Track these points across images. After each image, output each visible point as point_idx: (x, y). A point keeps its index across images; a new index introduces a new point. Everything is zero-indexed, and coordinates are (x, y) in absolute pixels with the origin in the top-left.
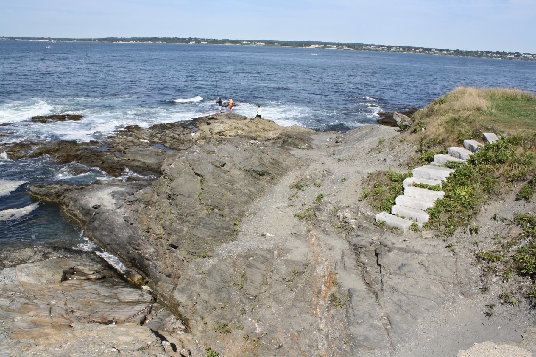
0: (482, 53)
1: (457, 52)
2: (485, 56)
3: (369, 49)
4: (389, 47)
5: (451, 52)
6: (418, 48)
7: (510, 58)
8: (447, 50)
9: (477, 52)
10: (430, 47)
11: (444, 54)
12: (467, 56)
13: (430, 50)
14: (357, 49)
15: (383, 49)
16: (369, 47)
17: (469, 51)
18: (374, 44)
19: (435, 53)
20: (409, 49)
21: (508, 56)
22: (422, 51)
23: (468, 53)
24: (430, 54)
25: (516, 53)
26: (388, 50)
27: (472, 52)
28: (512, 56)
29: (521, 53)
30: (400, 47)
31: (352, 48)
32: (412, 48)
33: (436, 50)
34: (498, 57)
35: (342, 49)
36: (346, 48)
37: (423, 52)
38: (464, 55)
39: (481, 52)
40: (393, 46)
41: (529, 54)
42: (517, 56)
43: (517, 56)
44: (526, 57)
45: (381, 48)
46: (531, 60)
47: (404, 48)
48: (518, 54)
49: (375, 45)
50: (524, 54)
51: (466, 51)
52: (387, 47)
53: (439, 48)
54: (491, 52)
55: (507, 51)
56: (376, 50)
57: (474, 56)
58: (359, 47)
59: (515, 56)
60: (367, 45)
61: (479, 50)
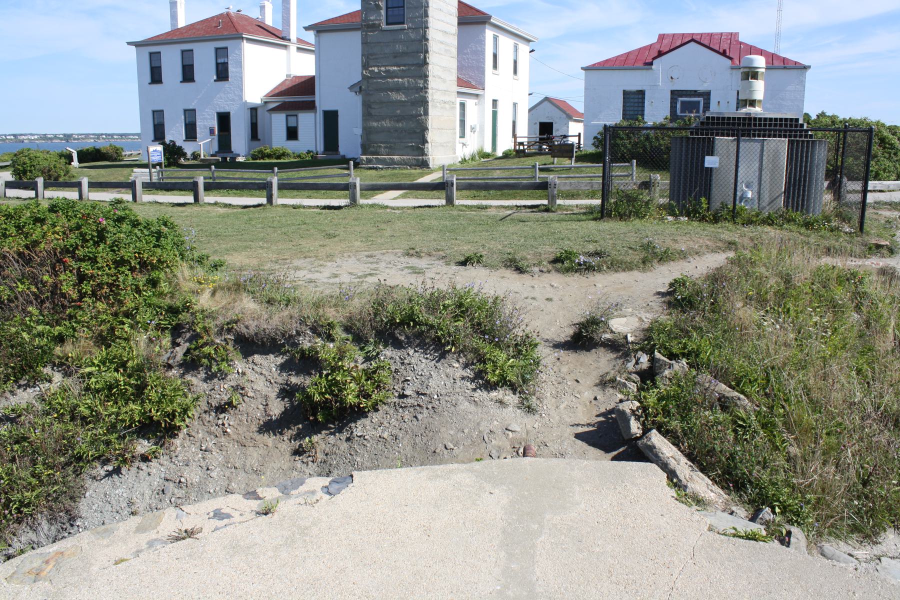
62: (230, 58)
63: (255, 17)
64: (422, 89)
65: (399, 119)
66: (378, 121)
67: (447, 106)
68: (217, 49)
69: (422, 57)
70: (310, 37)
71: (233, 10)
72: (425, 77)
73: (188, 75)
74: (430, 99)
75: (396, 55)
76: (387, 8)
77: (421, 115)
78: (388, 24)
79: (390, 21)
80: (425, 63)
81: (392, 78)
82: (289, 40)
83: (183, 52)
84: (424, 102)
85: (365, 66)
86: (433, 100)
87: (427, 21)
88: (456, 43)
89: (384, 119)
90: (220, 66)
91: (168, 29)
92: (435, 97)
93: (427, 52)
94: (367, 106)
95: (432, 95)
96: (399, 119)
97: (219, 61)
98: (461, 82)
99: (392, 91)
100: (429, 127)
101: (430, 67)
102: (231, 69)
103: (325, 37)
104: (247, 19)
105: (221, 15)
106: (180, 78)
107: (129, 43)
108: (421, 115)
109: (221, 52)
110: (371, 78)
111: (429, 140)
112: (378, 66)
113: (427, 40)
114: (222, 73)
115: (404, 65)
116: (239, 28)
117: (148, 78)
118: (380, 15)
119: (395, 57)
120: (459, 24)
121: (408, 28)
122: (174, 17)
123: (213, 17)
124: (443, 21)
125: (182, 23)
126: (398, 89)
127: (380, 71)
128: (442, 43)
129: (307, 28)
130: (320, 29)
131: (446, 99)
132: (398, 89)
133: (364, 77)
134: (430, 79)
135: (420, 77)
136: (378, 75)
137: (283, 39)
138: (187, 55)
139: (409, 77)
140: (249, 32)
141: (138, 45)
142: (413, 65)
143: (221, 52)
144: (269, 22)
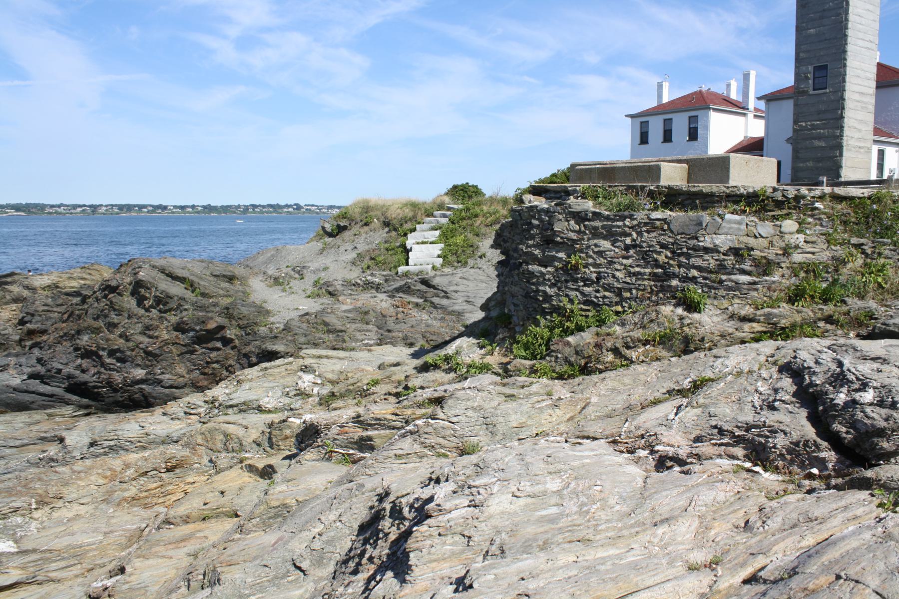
0: (246, 208)
1: (208, 209)
2: (251, 213)
3: (57, 213)
4: (94, 208)
5: (200, 208)
6: (145, 206)
7: (288, 212)
8: (193, 207)
9: (239, 206)
10: (164, 204)
11: (188, 212)
12: (224, 213)
13: (164, 208)
14: (35, 213)
15: (83, 210)
16: (57, 209)
17: (227, 206)
18: (65, 203)
19: (173, 213)
20: (129, 208)
21: (285, 210)
22: (152, 211)
23: (226, 209)
24: (166, 214)
25: (295, 204)
26: (93, 212)
27: (230, 206)
28: (291, 209)
29: (302, 204)
30: (112, 206)
31: (24, 211)
32: (135, 206)
33: (175, 207)
34: (271, 212)
35: (4, 215)
36: (13, 212)
37: (153, 211)
38: (219, 213)
39: (244, 206)
40: (101, 205)
41: (313, 206)
42: (296, 209)
43: (296, 209)
44: (310, 210)
45: (79, 209)
46: (317, 213)
47: (121, 207)
48: (298, 207)
49: (67, 206)
50: (306, 205)
51: (222, 207)
52: (90, 206)
53: (178, 204)
54: (260, 206)
55: (283, 203)
56: (71, 213)
57: (235, 212)
58: (39, 210)
59: (294, 209)
60: (52, 206)
61: (242, 204)
62: (699, 123)
63: (721, 93)
64: (838, 136)
65: (818, 160)
66: (804, 162)
67: (862, 150)
68: (690, 117)
69: (840, 112)
70: (762, 105)
71: (704, 88)
72: (841, 128)
73: (668, 137)
74: (845, 144)
75: (819, 112)
76: (814, 78)
77: (837, 156)
78: (814, 90)
79: (817, 86)
80: (842, 117)
81: (816, 129)
82: (748, 109)
83: (665, 120)
84: (840, 147)
85: (796, 122)
86: (848, 145)
87: (844, 86)
88: (873, 101)
89: (808, 161)
90: (692, 130)
91: (654, 104)
92: (850, 142)
93: (843, 108)
94: (796, 151)
95: (847, 141)
96: (818, 160)
97: (691, 126)
98: (877, 131)
99: (815, 139)
100: (843, 165)
101: (846, 120)
102: (700, 132)
103: (774, 104)
104: (715, 95)
105: (695, 93)
106: (662, 140)
107: (627, 116)
108: (837, 156)
109: (693, 120)
110: (800, 130)
111: (842, 175)
112: (805, 122)
113: (844, 100)
114: (693, 135)
115: (825, 120)
116: (708, 101)
117: (638, 141)
118: (809, 84)
119: (819, 114)
120: (877, 87)
121: (830, 92)
122: (660, 96)
123: (689, 95)
124: (859, 85)
125: (665, 99)
126: (819, 137)
127: (807, 125)
128: (858, 101)
129: (759, 99)
130: (771, 98)
131: (862, 144)
132: (819, 137)
133: (795, 131)
134: (845, 129)
135: (837, 128)
136: (805, 129)
137: (743, 108)
138: (668, 123)
139: (828, 128)
140: (715, 104)
141: (632, 116)
142: (832, 119)
143: (693, 120)
144: (734, 96)
